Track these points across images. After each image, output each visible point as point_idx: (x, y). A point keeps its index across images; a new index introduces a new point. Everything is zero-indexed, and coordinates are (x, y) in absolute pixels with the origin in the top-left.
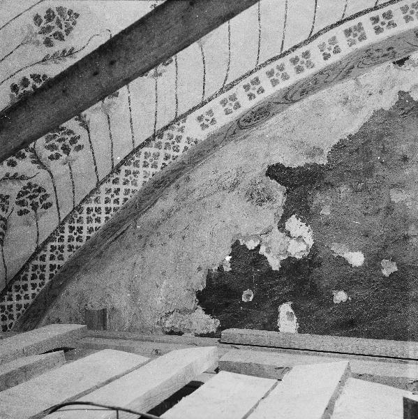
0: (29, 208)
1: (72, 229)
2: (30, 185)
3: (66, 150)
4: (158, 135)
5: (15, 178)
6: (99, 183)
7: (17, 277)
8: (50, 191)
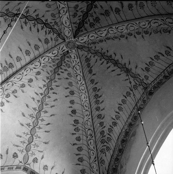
2: (107, 147)
3: (110, 140)
4: (120, 134)
6: (116, 144)
8: (110, 147)
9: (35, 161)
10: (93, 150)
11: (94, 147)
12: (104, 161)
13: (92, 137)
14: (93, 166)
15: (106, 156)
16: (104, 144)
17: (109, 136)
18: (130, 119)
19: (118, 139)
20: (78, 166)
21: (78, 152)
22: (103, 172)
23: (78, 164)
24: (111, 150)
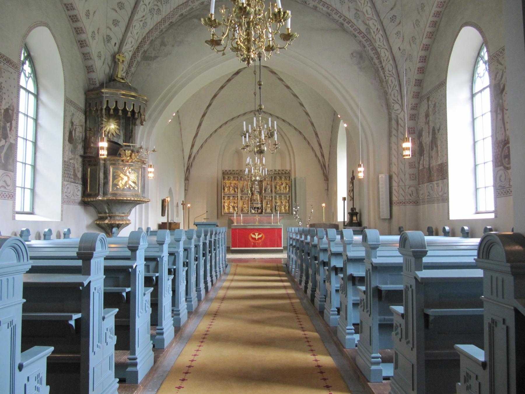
1: (164, 21)
3: (166, 3)
5: (157, 6)
6: (171, 12)
7: (151, 30)
8: (162, 11)
10: (146, 5)
11: (149, 3)
12: (146, 25)
14: (135, 26)
15: (151, 19)
16: (158, 2)
19: (176, 8)
20: (114, 12)
23: (115, 10)
24: (161, 16)
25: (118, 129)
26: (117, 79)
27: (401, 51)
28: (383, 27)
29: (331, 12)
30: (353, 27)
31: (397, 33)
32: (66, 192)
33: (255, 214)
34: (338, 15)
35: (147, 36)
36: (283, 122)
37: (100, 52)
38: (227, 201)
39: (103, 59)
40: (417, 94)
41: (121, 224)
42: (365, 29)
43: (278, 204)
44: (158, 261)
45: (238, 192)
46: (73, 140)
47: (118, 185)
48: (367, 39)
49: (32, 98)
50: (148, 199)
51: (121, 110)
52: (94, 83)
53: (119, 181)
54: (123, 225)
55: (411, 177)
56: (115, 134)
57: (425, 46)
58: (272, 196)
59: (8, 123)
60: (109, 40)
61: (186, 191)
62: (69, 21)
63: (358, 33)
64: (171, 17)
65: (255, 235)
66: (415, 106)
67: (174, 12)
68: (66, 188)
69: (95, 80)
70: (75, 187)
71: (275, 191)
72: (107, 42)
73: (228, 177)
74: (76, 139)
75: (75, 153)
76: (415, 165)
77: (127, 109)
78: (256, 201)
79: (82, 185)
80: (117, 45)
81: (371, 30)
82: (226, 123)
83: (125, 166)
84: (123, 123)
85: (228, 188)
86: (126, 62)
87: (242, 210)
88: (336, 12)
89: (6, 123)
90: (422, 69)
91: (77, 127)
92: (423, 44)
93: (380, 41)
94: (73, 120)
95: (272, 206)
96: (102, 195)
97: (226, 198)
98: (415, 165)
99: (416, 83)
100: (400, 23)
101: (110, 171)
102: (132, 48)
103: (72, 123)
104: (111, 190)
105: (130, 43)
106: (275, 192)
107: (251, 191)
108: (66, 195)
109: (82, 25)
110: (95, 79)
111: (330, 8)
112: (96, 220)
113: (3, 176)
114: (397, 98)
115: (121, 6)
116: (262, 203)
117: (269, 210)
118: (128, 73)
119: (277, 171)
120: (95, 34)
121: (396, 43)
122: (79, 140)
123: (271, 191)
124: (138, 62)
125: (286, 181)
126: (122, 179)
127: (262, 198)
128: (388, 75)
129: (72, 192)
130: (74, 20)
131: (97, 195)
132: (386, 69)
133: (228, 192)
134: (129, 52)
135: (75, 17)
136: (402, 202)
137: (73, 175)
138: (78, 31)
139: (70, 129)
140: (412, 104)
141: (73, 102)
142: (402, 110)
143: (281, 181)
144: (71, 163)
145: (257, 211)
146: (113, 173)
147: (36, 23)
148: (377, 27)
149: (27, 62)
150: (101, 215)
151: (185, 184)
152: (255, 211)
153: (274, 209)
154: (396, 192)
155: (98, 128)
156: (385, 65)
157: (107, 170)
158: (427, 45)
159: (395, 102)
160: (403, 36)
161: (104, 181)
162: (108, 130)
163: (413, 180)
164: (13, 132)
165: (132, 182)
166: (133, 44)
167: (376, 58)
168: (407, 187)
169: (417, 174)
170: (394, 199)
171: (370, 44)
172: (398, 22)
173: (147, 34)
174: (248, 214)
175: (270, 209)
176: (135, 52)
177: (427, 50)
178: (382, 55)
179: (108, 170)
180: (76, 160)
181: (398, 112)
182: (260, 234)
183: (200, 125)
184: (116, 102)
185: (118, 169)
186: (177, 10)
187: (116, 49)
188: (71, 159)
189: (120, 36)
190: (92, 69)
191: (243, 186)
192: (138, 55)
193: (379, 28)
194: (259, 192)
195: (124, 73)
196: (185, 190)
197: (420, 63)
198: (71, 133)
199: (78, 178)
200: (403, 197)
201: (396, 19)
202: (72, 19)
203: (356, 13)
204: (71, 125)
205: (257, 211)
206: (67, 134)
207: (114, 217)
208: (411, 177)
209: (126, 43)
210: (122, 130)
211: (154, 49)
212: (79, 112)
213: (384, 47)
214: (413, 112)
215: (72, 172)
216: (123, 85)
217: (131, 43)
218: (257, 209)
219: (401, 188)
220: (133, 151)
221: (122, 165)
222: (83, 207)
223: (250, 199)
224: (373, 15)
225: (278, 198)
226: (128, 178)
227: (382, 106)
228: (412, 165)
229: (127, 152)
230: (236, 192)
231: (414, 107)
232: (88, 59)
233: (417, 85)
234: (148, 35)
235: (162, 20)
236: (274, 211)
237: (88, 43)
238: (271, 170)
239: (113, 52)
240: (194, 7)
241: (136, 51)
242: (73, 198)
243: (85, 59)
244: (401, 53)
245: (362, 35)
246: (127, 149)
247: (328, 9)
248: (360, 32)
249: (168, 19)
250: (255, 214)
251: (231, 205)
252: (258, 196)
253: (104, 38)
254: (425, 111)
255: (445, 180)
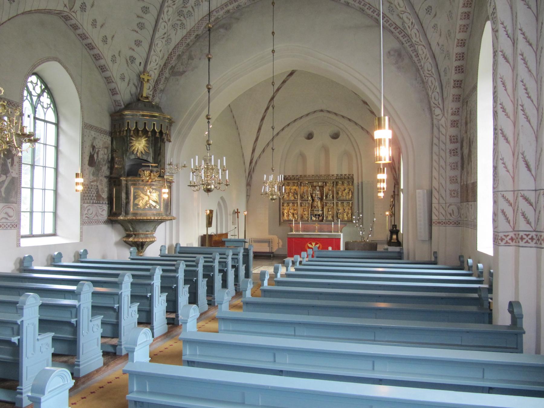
0: (181, 28)
1: (189, 34)
5: (180, 20)
6: (195, 25)
7: (177, 45)
8: (186, 25)
9: (83, 8)
10: (166, 22)
12: (171, 41)
13: (174, 4)
14: (157, 44)
15: (176, 34)
16: (180, 17)
17: (191, 10)
18: (232, 5)
19: (201, 20)
21: (140, 13)
22: (164, 54)
23: (136, 31)
25: (147, 147)
26: (141, 99)
27: (440, 47)
28: (420, 20)
29: (363, 7)
30: (388, 21)
31: (434, 26)
32: (87, 214)
33: (316, 221)
34: (372, 10)
35: (174, 52)
36: (349, 122)
37: (123, 74)
38: (286, 208)
39: (127, 80)
40: (458, 97)
41: (145, 242)
42: (401, 24)
43: (340, 211)
44: (77, 309)
45: (297, 199)
46: (95, 163)
47: (138, 205)
48: (404, 35)
49: (52, 129)
50: (171, 217)
51: (141, 131)
52: (119, 104)
53: (139, 201)
54: (146, 243)
55: (452, 194)
56: (143, 152)
57: (460, 42)
58: (334, 203)
59: (8, 159)
60: (133, 61)
61: (248, 197)
62: (86, 49)
63: (394, 28)
64: (196, 29)
65: (312, 245)
66: (456, 110)
67: (199, 24)
68: (86, 210)
69: (120, 102)
70: (98, 208)
71: (337, 197)
72: (131, 63)
73: (288, 183)
74: (99, 162)
75: (98, 175)
76: (456, 179)
77: (148, 129)
78: (317, 208)
79: (108, 204)
80: (143, 65)
81: (406, 25)
82: (288, 125)
83: (146, 185)
84: (152, 141)
85: (288, 194)
86: (152, 80)
87: (302, 217)
88: (369, 7)
89: (7, 159)
90: (460, 68)
91: (100, 149)
92: (457, 39)
93: (416, 36)
94: (94, 144)
95: (333, 213)
96: (124, 214)
97: (285, 205)
98: (456, 179)
99: (455, 84)
100: (435, 15)
101: (131, 191)
102: (158, 66)
103: (93, 147)
104: (132, 210)
105: (154, 61)
106: (337, 199)
107: (312, 197)
108: (86, 217)
109: (98, 52)
110: (119, 101)
111: (362, 4)
112: (123, 238)
113: (3, 209)
114: (438, 101)
115: (142, 26)
116: (323, 210)
117: (330, 218)
118: (157, 91)
119: (339, 175)
120: (116, 58)
121: (434, 38)
122: (104, 161)
123: (333, 197)
124: (166, 78)
125: (349, 187)
126: (143, 199)
127: (323, 205)
128: (428, 75)
129: (94, 213)
130: (90, 48)
131: (120, 214)
132: (426, 68)
133: (288, 198)
134: (154, 70)
135: (90, 45)
136: (442, 222)
137: (95, 196)
138: (97, 57)
139: (91, 153)
140: (452, 109)
141: (94, 126)
142: (444, 115)
143: (343, 187)
144: (92, 185)
145: (318, 218)
146: (134, 193)
147: (41, 60)
148: (411, 21)
149: (45, 94)
150: (127, 232)
151: (247, 190)
152: (316, 218)
153: (336, 216)
154: (436, 210)
155: (127, 147)
156: (424, 64)
157: (128, 191)
158: (462, 40)
159: (435, 106)
160: (441, 30)
161: (126, 200)
162: (136, 149)
163: (454, 197)
164: (16, 167)
165: (153, 201)
166: (157, 62)
167: (415, 55)
168: (448, 205)
169: (459, 190)
170: (434, 218)
171: (408, 40)
172: (434, 13)
173: (173, 50)
174: (308, 221)
175: (331, 216)
176: (162, 69)
177: (464, 46)
178: (420, 52)
179: (129, 191)
180: (99, 181)
181: (439, 117)
182: (318, 244)
183: (260, 129)
184: (136, 123)
185: (138, 189)
186: (202, 21)
187: (141, 68)
188: (92, 182)
189: (145, 55)
190: (116, 91)
191: (303, 192)
192: (165, 71)
193: (414, 21)
194: (320, 198)
195: (151, 91)
196: (247, 196)
197: (456, 61)
198: (91, 157)
199: (103, 198)
200: (444, 216)
201: (431, 10)
202: (88, 47)
203: (390, 6)
204: (91, 149)
205: (318, 218)
206: (87, 158)
207: (138, 235)
208: (452, 194)
209: (151, 62)
210: (152, 148)
211: (182, 65)
212: (102, 135)
213: (421, 43)
214: (455, 118)
215: (94, 193)
216: (145, 106)
217: (156, 61)
218: (318, 216)
219: (441, 206)
220: (151, 171)
221: (143, 185)
222: (110, 225)
223: (310, 205)
224: (405, 7)
225: (339, 205)
226: (149, 197)
227: (423, 110)
228: (453, 180)
229: (145, 172)
230: (295, 198)
231: (455, 112)
232: (110, 82)
233: (457, 87)
234: (174, 51)
235: (187, 34)
236: (335, 218)
237: (107, 67)
238: (333, 175)
239: (138, 72)
240: (220, 17)
241: (163, 68)
242: (96, 218)
243: (108, 83)
244: (440, 49)
245: (399, 29)
246: (145, 169)
247: (360, 4)
248: (396, 27)
249: (193, 32)
250: (316, 221)
251: (290, 212)
252: (319, 202)
253: (127, 60)
254: (465, 117)
255: (476, 203)
